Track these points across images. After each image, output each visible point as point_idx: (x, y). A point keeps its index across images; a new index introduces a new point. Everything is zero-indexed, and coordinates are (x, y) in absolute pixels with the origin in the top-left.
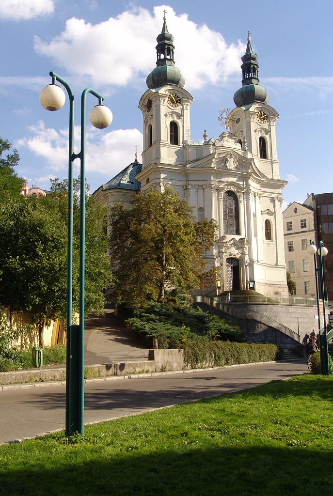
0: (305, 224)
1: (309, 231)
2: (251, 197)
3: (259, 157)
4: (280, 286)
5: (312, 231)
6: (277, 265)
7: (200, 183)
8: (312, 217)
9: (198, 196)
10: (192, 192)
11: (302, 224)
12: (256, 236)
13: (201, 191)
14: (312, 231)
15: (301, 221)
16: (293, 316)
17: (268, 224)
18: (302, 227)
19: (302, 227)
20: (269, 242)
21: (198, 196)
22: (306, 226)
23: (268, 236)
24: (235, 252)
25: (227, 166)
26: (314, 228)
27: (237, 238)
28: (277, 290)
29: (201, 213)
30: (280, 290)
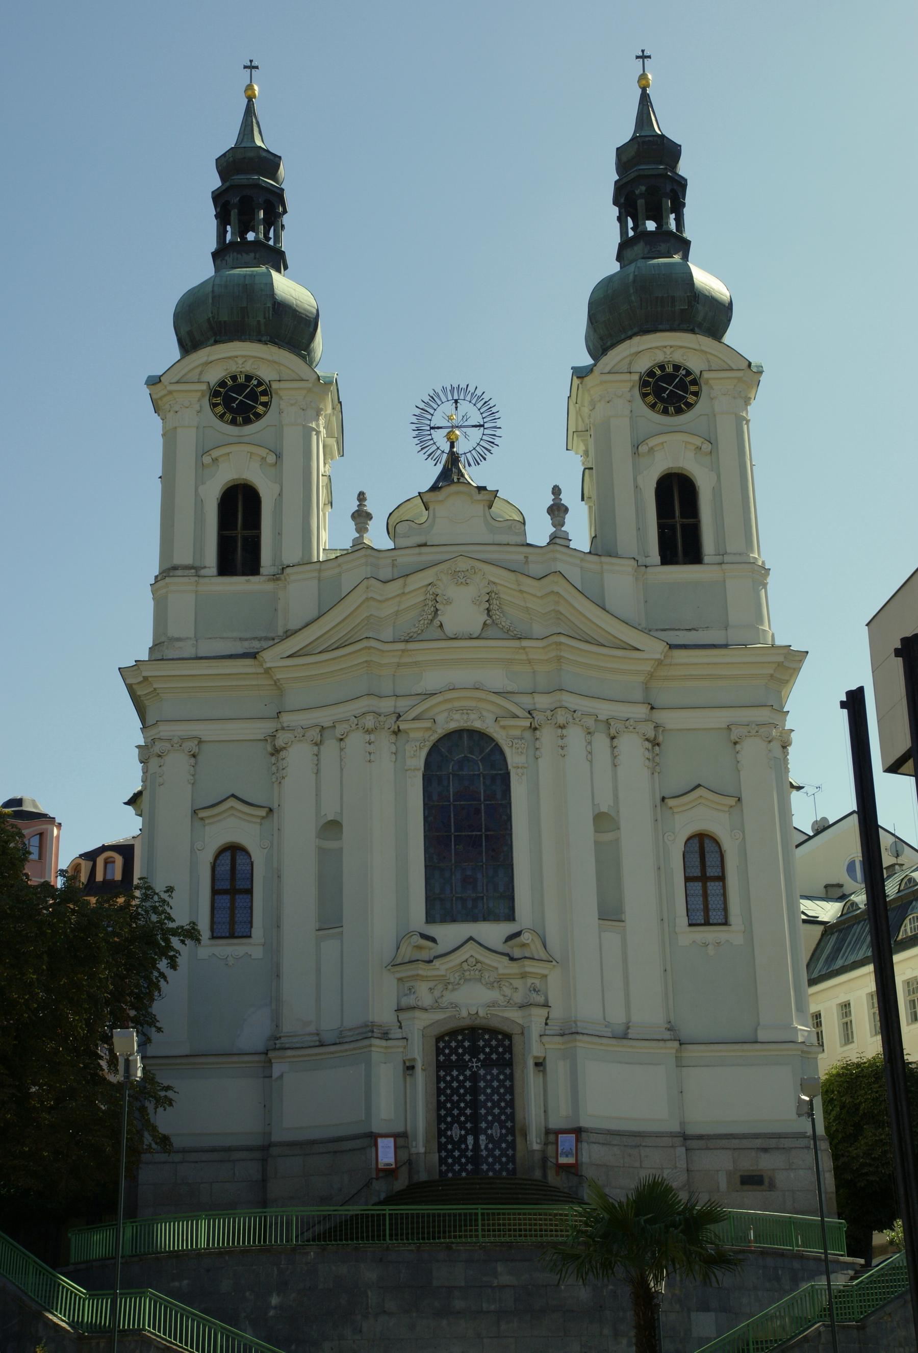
2: (575, 736)
3: (657, 559)
4: (770, 1141)
6: (756, 1042)
7: (325, 717)
9: (317, 773)
10: (298, 756)
16: (459, 1304)
21: (317, 773)
24: (474, 1001)
25: (441, 626)
27: (492, 932)
28: (747, 1164)
29: (331, 845)
30: (765, 1163)
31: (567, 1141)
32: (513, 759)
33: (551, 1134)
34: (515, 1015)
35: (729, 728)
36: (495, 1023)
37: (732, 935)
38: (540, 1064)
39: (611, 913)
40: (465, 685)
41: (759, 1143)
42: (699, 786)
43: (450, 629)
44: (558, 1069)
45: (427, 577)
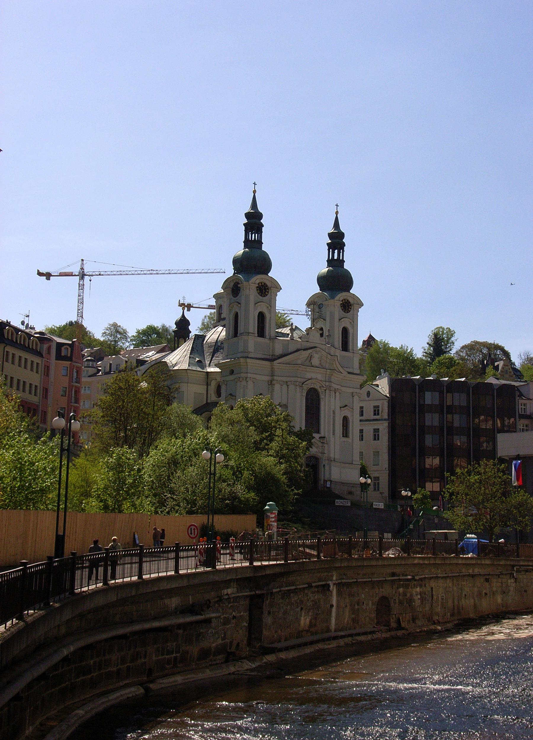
0: (378, 410)
1: (382, 420)
5: (385, 420)
7: (285, 379)
8: (386, 404)
10: (277, 387)
11: (375, 411)
12: (334, 434)
13: (285, 387)
14: (385, 420)
15: (375, 407)
17: (345, 420)
18: (375, 414)
19: (375, 414)
20: (345, 439)
22: (378, 414)
23: (346, 434)
26: (386, 417)
31: (329, 483)
32: (322, 396)
33: (325, 481)
34: (320, 455)
35: (352, 393)
36: (316, 456)
37: (349, 440)
38: (324, 466)
39: (334, 434)
40: (316, 377)
41: (352, 485)
42: (346, 406)
43: (313, 364)
44: (327, 467)
45: (310, 351)
